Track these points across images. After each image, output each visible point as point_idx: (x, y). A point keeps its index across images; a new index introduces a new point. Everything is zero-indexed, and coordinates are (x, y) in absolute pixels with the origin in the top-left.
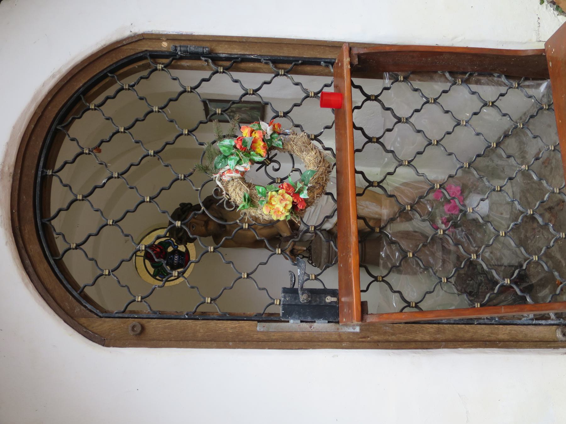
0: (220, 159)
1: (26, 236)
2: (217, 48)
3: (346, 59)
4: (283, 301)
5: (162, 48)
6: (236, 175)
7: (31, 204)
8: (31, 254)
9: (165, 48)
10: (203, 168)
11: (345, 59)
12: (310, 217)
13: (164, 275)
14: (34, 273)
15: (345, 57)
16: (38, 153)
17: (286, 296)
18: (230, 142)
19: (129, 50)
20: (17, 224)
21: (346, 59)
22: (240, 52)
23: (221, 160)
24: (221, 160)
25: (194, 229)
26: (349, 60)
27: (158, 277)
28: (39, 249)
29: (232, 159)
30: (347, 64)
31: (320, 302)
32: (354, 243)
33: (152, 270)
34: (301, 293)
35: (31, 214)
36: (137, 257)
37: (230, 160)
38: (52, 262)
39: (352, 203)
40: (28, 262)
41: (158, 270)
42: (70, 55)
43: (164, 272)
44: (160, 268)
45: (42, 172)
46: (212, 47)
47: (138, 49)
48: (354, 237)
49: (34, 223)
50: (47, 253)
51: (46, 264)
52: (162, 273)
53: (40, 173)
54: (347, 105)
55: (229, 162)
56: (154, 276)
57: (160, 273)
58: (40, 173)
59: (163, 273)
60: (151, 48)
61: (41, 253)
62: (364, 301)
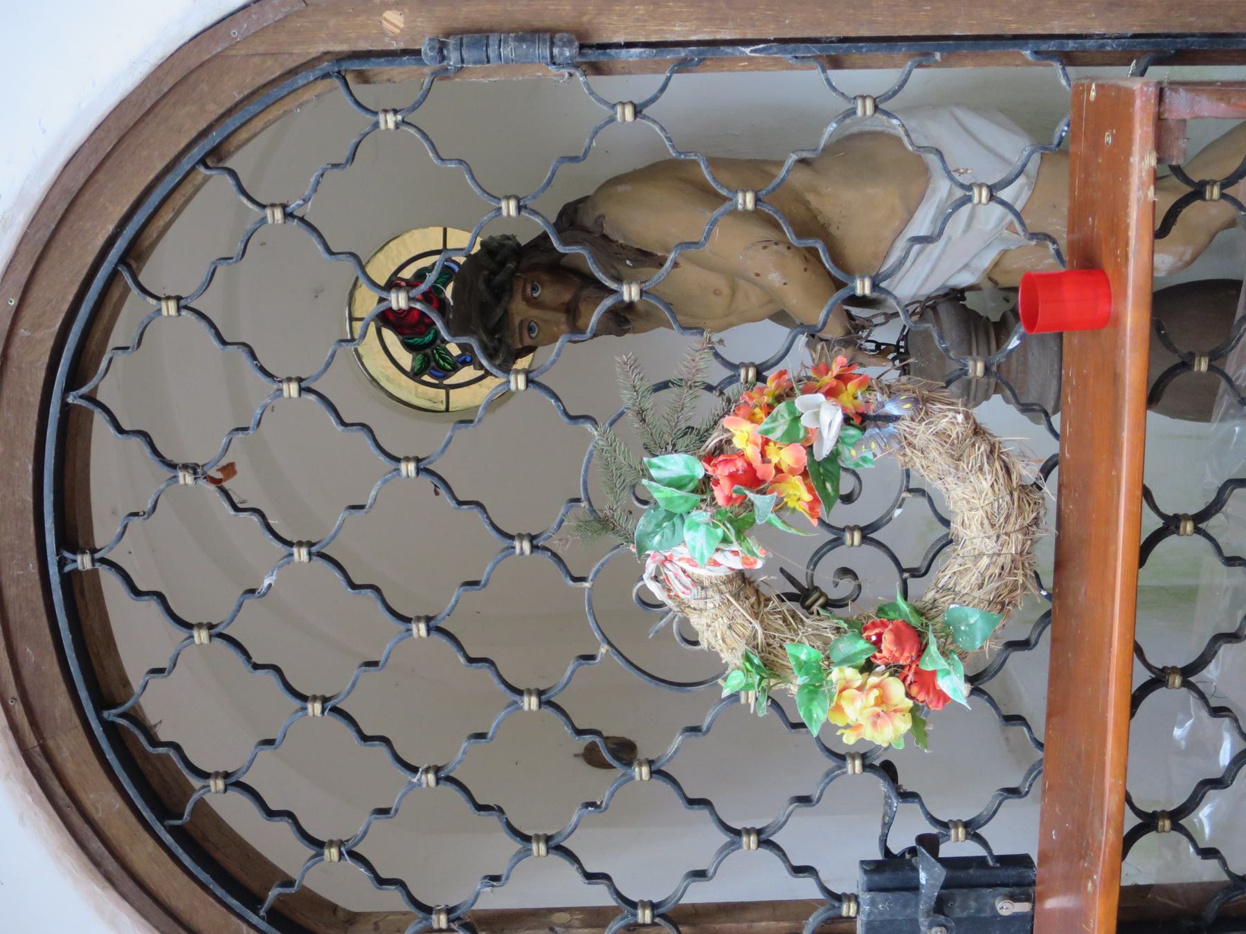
0: (654, 522)
1: (70, 769)
2: (604, 19)
3: (1142, 159)
4: (869, 915)
5: (387, 39)
6: (713, 574)
7: (56, 669)
8: (98, 816)
9: (395, 38)
10: (562, 271)
11: (1135, 159)
12: (908, 263)
13: (443, 369)
14: (124, 875)
15: (1136, 148)
16: (29, 499)
17: (878, 899)
18: (687, 467)
19: (257, 60)
20: (31, 740)
21: (1142, 159)
22: (695, 32)
23: (659, 525)
24: (659, 525)
25: (533, 335)
26: (1153, 162)
27: (426, 378)
28: (118, 804)
29: (698, 524)
30: (1142, 184)
31: (979, 910)
32: (1108, 849)
33: (406, 359)
34: (926, 923)
35: (64, 701)
36: (354, 323)
37: (689, 529)
38: (168, 839)
39: (1116, 724)
40: (96, 845)
41: (426, 355)
42: (44, 131)
43: (444, 360)
44: (428, 351)
45: (62, 563)
46: (585, 19)
47: (291, 54)
48: (1111, 831)
49: (80, 728)
50: (147, 814)
51: (151, 843)
52: (437, 363)
53: (53, 570)
54: (1128, 361)
55: (688, 535)
56: (415, 375)
57: (433, 364)
58: (53, 570)
59: (437, 357)
60: (341, 43)
61: (128, 812)
62: (1121, 910)
